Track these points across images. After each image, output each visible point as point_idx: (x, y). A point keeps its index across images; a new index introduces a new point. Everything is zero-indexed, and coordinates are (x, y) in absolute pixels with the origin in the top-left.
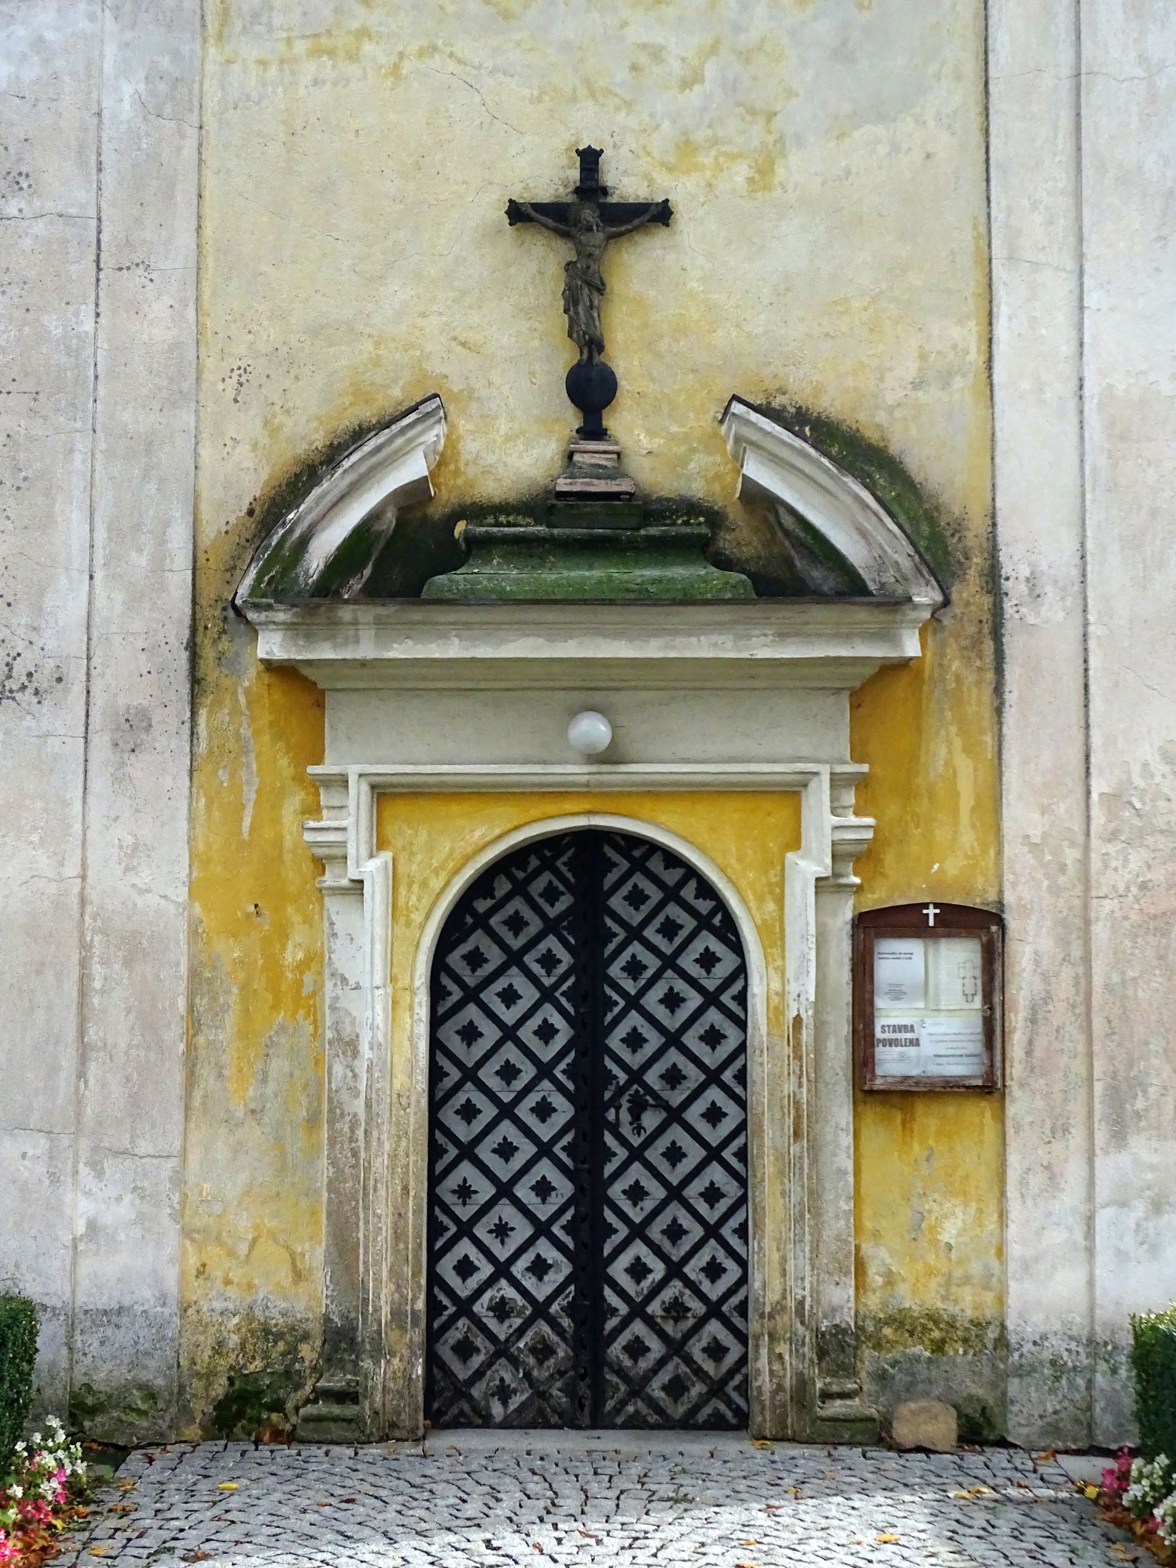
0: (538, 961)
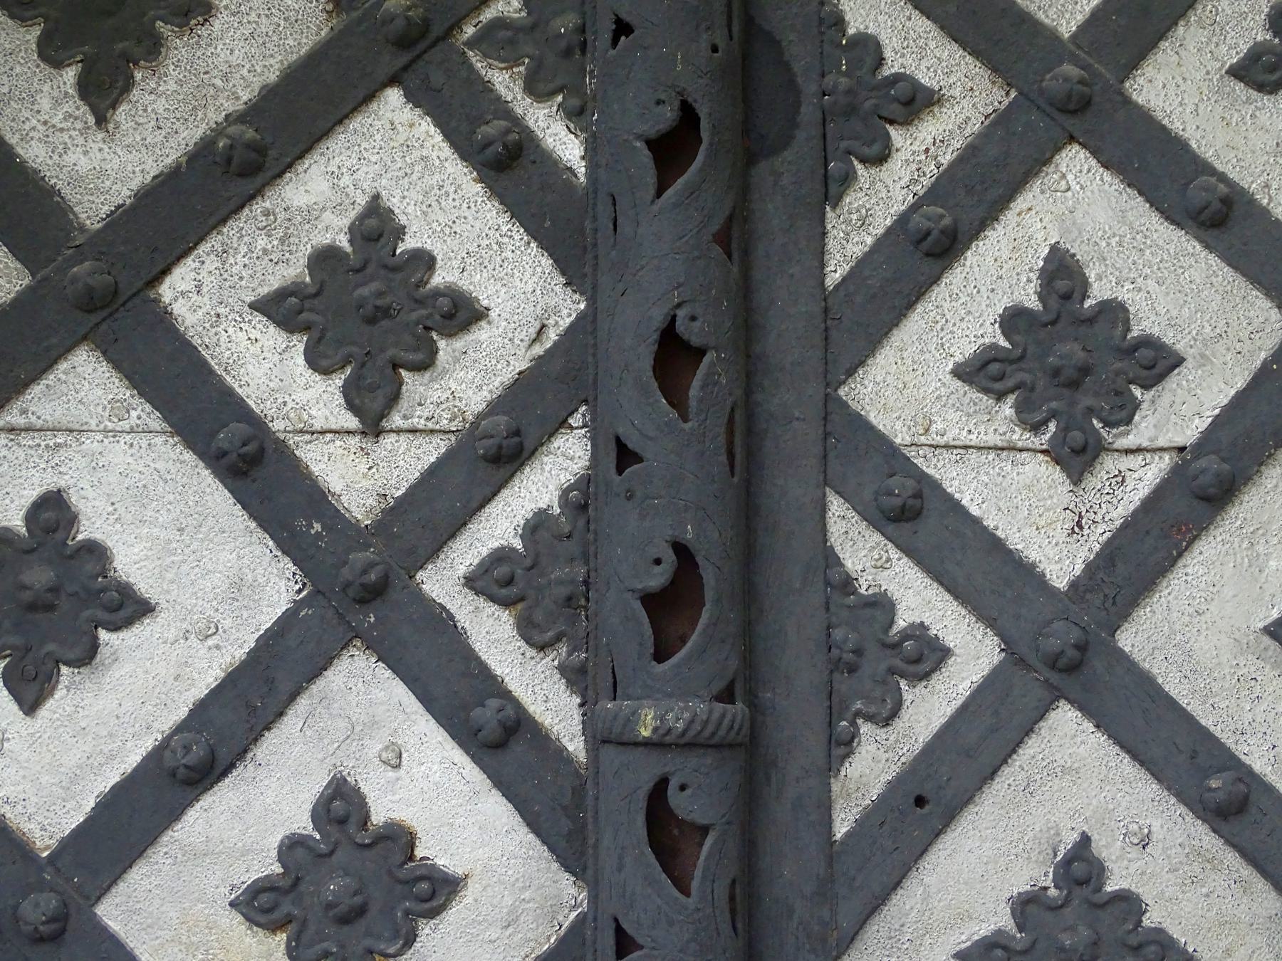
0: (281, 308)
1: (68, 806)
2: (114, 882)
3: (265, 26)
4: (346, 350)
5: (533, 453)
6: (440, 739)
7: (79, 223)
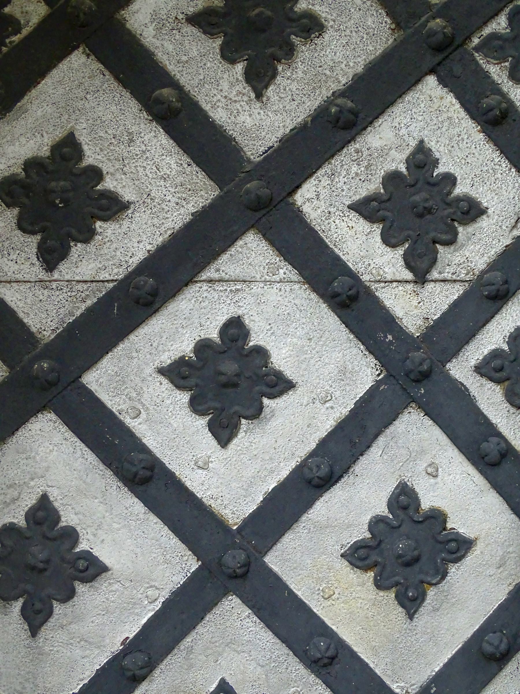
1: (247, 500)
2: (275, 543)
3: (355, 38)
4: (406, 233)
5: (514, 294)
6: (460, 460)
7: (247, 158)
